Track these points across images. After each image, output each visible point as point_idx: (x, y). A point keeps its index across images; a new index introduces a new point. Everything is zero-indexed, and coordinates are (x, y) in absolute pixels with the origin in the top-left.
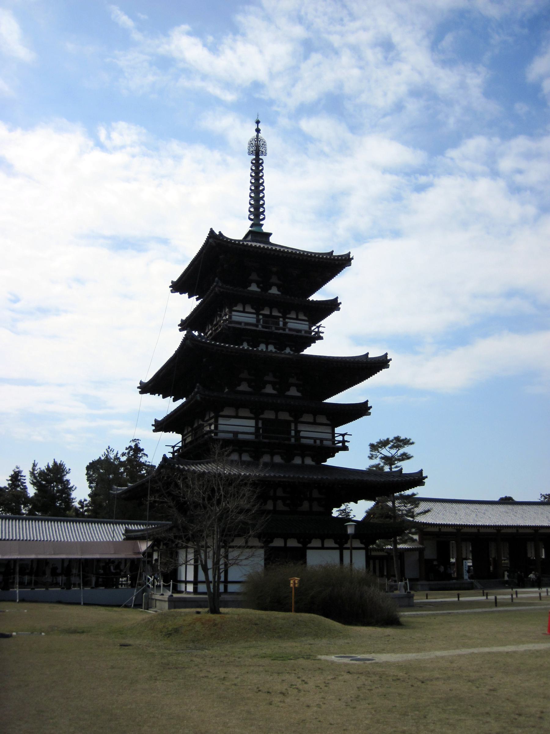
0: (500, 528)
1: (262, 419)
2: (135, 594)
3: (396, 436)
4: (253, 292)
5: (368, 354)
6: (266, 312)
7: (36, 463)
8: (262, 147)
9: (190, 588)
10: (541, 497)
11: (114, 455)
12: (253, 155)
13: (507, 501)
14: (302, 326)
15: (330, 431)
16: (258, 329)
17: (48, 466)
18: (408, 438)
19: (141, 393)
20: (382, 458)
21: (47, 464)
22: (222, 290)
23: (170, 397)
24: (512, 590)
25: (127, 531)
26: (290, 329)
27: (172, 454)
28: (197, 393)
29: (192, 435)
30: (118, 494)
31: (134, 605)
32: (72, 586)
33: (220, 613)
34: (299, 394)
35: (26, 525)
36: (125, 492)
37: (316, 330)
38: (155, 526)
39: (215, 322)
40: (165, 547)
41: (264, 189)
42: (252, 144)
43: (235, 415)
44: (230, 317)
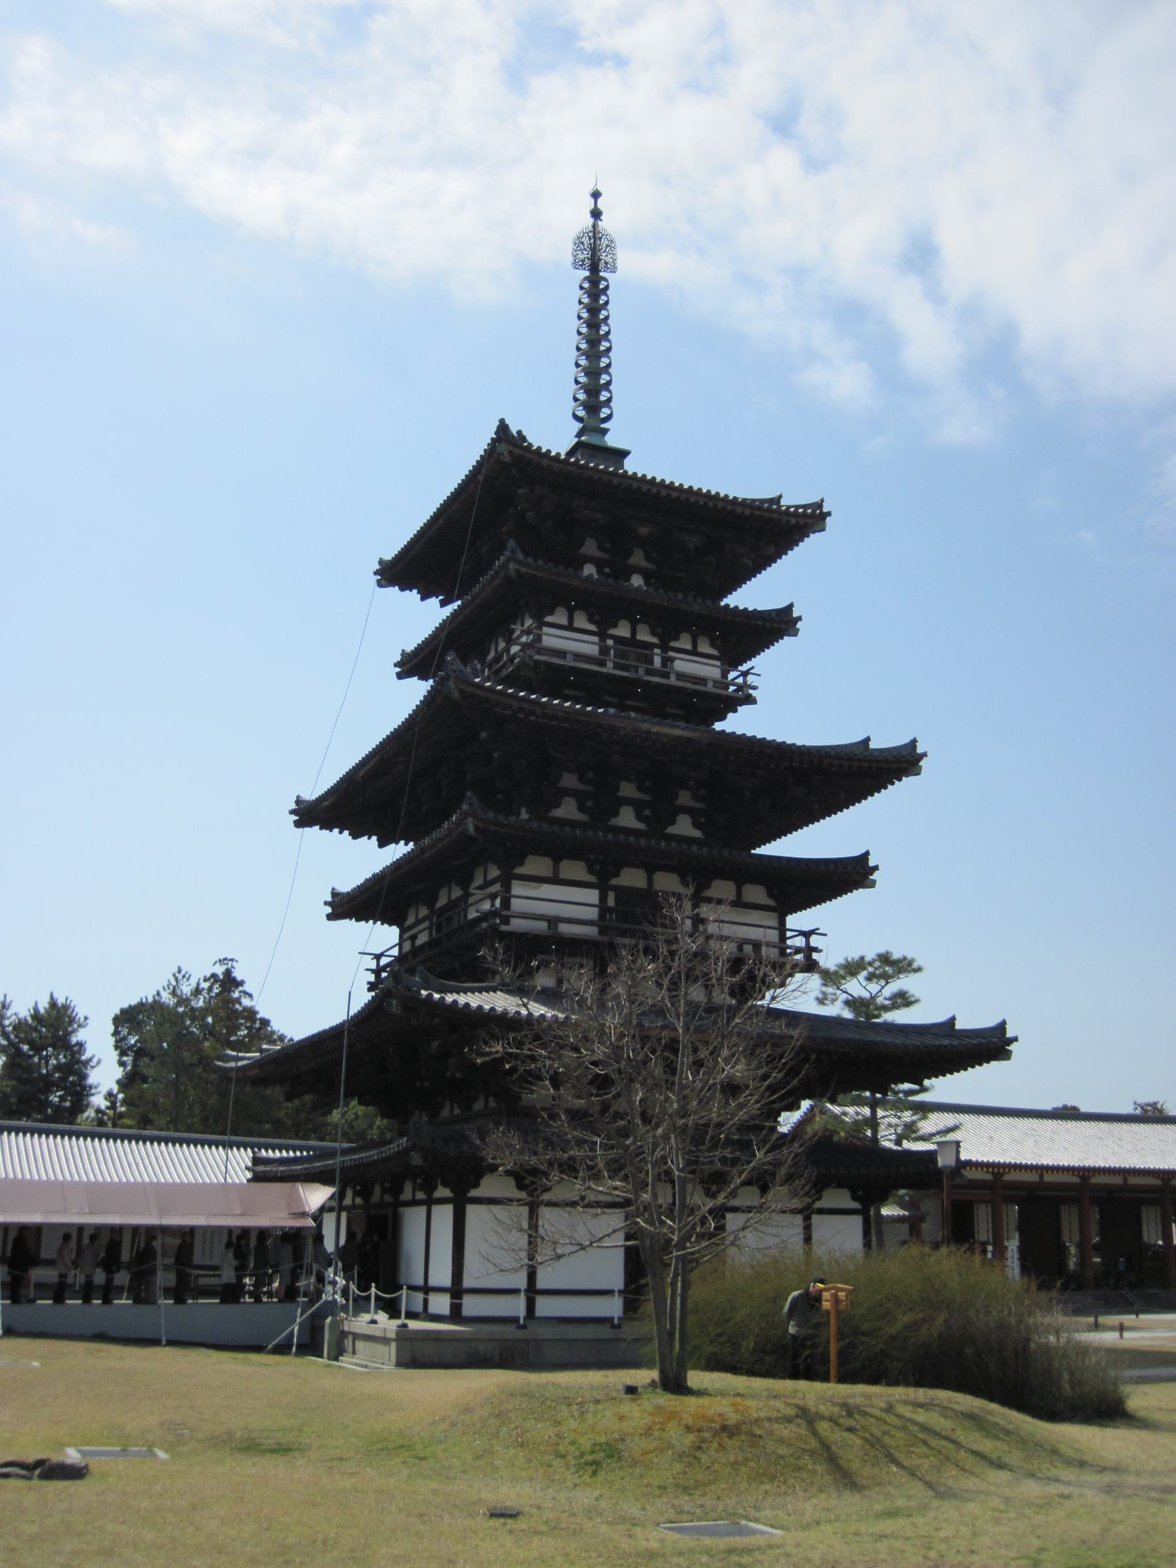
0: (1086, 1174)
1: (615, 888)
2: (298, 1320)
3: (882, 950)
5: (868, 739)
6: (623, 630)
7: (8, 1001)
8: (605, 252)
9: (441, 1304)
10: (1136, 1108)
11: (190, 987)
12: (585, 269)
13: (1068, 1114)
14: (710, 670)
15: (774, 923)
16: (604, 670)
17: (36, 1009)
18: (909, 957)
19: (298, 824)
20: (847, 1003)
21: (33, 1004)
22: (524, 570)
23: (367, 837)
24: (1137, 1316)
25: (256, 1161)
26: (681, 676)
27: (373, 975)
28: (467, 815)
29: (430, 928)
30: (239, 1069)
31: (299, 1346)
32: (126, 1293)
33: (689, 1392)
34: (697, 834)
35: (9, 1141)
36: (256, 1064)
37: (740, 680)
38: (308, 1152)
39: (492, 655)
40: (359, 1201)
41: (609, 349)
42: (582, 243)
43: (552, 876)
44: (539, 639)
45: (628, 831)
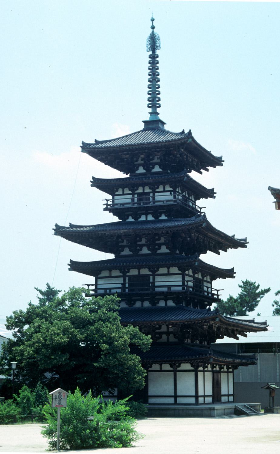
4: (140, 174)
6: (140, 190)
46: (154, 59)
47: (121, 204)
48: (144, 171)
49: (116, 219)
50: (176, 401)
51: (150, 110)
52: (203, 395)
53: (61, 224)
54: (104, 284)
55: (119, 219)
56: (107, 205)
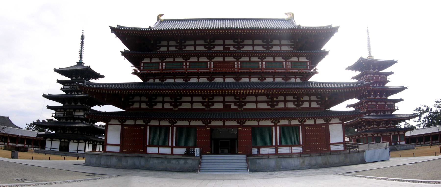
6: (73, 84)
45: (73, 105)
46: (82, 43)
47: (66, 89)
48: (75, 78)
49: (64, 93)
50: (78, 152)
51: (79, 59)
52: (88, 151)
53: (45, 94)
54: (59, 113)
55: (65, 93)
56: (61, 88)
